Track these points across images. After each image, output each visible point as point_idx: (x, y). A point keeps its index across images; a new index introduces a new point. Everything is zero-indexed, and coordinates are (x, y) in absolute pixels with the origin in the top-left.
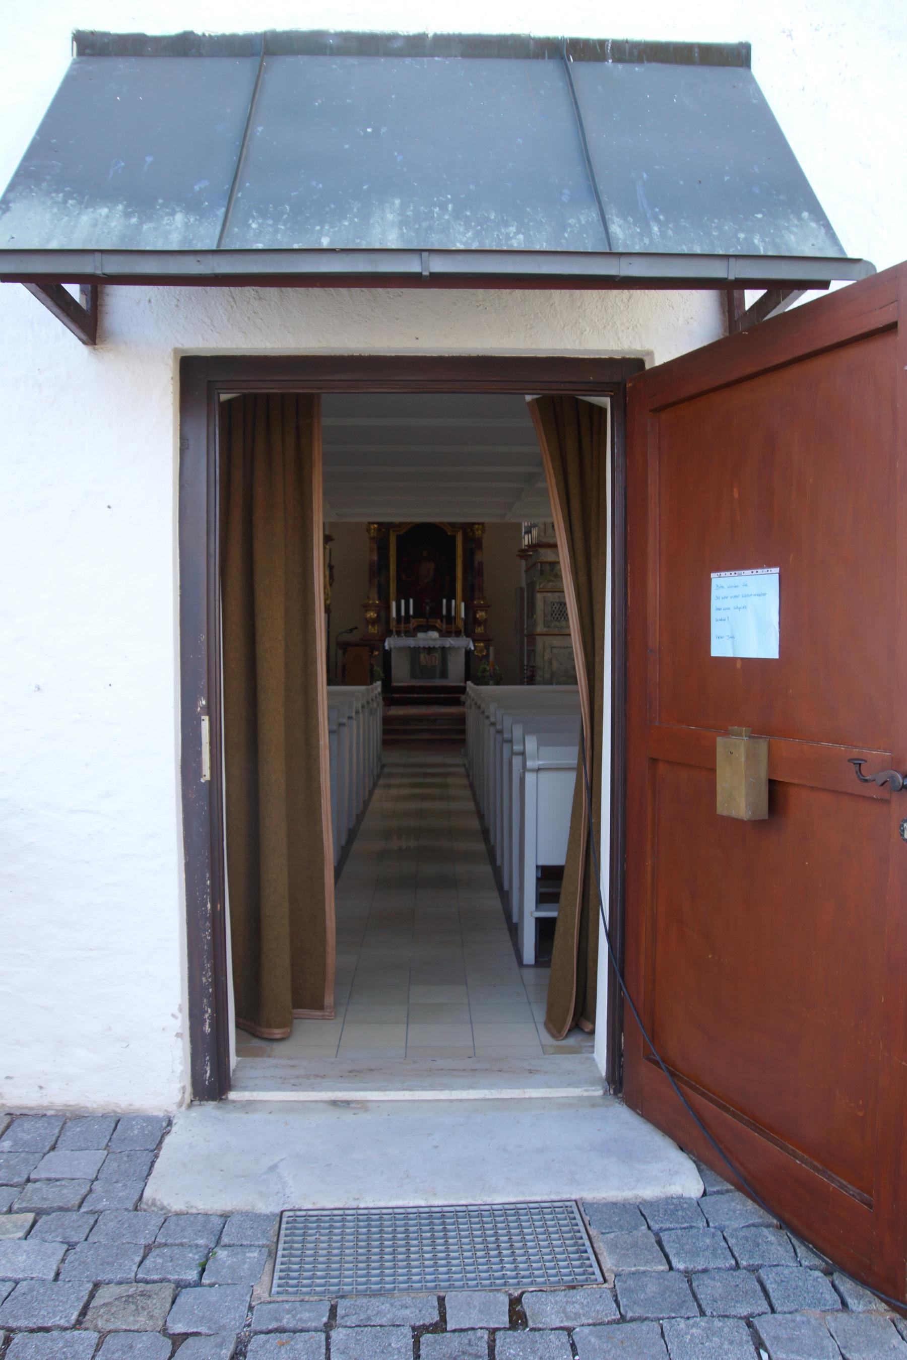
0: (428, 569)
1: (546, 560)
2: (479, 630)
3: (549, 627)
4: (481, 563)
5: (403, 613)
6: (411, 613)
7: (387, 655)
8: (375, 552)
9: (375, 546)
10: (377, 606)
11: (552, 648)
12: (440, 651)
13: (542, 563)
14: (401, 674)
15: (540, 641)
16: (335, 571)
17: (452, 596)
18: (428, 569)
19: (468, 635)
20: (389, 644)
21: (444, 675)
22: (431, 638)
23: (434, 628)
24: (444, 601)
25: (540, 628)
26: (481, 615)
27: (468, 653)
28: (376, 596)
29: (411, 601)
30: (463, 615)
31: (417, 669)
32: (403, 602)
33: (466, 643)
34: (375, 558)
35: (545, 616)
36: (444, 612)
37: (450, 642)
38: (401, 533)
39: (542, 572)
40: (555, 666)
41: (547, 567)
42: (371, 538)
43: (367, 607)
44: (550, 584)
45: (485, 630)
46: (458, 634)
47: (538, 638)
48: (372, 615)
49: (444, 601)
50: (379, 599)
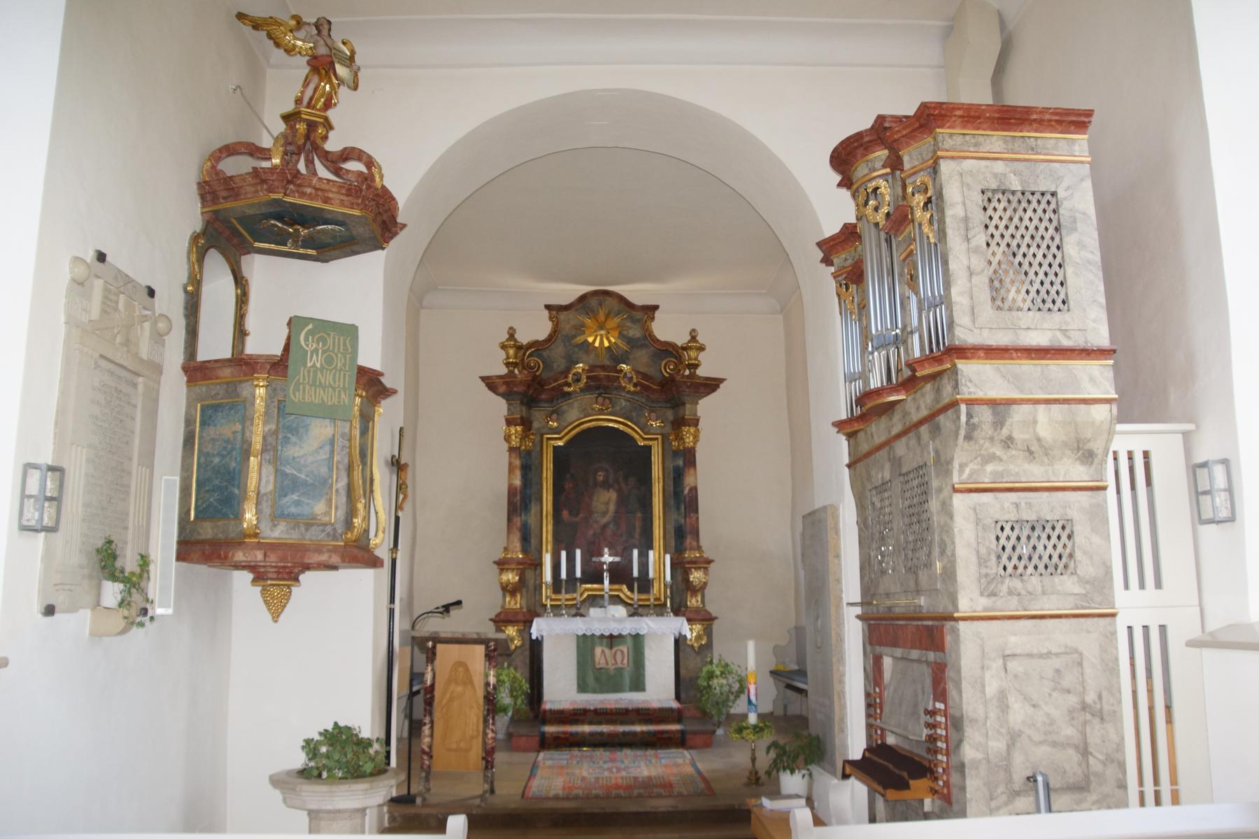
0: (605, 501)
1: (980, 395)
2: (693, 602)
4: (694, 490)
5: (564, 575)
6: (578, 574)
7: (535, 647)
8: (518, 473)
9: (517, 462)
10: (519, 562)
11: (1005, 657)
12: (630, 642)
13: (970, 402)
14: (561, 688)
17: (647, 544)
18: (605, 501)
19: (677, 612)
20: (538, 630)
22: (611, 619)
24: (635, 552)
25: (968, 600)
26: (696, 576)
27: (679, 642)
29: (578, 553)
30: (668, 578)
31: (589, 676)
32: (564, 554)
34: (517, 482)
35: (982, 562)
36: (636, 574)
38: (561, 443)
40: (1018, 713)
42: (511, 449)
43: (502, 565)
44: (990, 468)
45: (703, 602)
46: (659, 609)
47: (962, 625)
48: (511, 577)
49: (635, 552)
50: (524, 551)
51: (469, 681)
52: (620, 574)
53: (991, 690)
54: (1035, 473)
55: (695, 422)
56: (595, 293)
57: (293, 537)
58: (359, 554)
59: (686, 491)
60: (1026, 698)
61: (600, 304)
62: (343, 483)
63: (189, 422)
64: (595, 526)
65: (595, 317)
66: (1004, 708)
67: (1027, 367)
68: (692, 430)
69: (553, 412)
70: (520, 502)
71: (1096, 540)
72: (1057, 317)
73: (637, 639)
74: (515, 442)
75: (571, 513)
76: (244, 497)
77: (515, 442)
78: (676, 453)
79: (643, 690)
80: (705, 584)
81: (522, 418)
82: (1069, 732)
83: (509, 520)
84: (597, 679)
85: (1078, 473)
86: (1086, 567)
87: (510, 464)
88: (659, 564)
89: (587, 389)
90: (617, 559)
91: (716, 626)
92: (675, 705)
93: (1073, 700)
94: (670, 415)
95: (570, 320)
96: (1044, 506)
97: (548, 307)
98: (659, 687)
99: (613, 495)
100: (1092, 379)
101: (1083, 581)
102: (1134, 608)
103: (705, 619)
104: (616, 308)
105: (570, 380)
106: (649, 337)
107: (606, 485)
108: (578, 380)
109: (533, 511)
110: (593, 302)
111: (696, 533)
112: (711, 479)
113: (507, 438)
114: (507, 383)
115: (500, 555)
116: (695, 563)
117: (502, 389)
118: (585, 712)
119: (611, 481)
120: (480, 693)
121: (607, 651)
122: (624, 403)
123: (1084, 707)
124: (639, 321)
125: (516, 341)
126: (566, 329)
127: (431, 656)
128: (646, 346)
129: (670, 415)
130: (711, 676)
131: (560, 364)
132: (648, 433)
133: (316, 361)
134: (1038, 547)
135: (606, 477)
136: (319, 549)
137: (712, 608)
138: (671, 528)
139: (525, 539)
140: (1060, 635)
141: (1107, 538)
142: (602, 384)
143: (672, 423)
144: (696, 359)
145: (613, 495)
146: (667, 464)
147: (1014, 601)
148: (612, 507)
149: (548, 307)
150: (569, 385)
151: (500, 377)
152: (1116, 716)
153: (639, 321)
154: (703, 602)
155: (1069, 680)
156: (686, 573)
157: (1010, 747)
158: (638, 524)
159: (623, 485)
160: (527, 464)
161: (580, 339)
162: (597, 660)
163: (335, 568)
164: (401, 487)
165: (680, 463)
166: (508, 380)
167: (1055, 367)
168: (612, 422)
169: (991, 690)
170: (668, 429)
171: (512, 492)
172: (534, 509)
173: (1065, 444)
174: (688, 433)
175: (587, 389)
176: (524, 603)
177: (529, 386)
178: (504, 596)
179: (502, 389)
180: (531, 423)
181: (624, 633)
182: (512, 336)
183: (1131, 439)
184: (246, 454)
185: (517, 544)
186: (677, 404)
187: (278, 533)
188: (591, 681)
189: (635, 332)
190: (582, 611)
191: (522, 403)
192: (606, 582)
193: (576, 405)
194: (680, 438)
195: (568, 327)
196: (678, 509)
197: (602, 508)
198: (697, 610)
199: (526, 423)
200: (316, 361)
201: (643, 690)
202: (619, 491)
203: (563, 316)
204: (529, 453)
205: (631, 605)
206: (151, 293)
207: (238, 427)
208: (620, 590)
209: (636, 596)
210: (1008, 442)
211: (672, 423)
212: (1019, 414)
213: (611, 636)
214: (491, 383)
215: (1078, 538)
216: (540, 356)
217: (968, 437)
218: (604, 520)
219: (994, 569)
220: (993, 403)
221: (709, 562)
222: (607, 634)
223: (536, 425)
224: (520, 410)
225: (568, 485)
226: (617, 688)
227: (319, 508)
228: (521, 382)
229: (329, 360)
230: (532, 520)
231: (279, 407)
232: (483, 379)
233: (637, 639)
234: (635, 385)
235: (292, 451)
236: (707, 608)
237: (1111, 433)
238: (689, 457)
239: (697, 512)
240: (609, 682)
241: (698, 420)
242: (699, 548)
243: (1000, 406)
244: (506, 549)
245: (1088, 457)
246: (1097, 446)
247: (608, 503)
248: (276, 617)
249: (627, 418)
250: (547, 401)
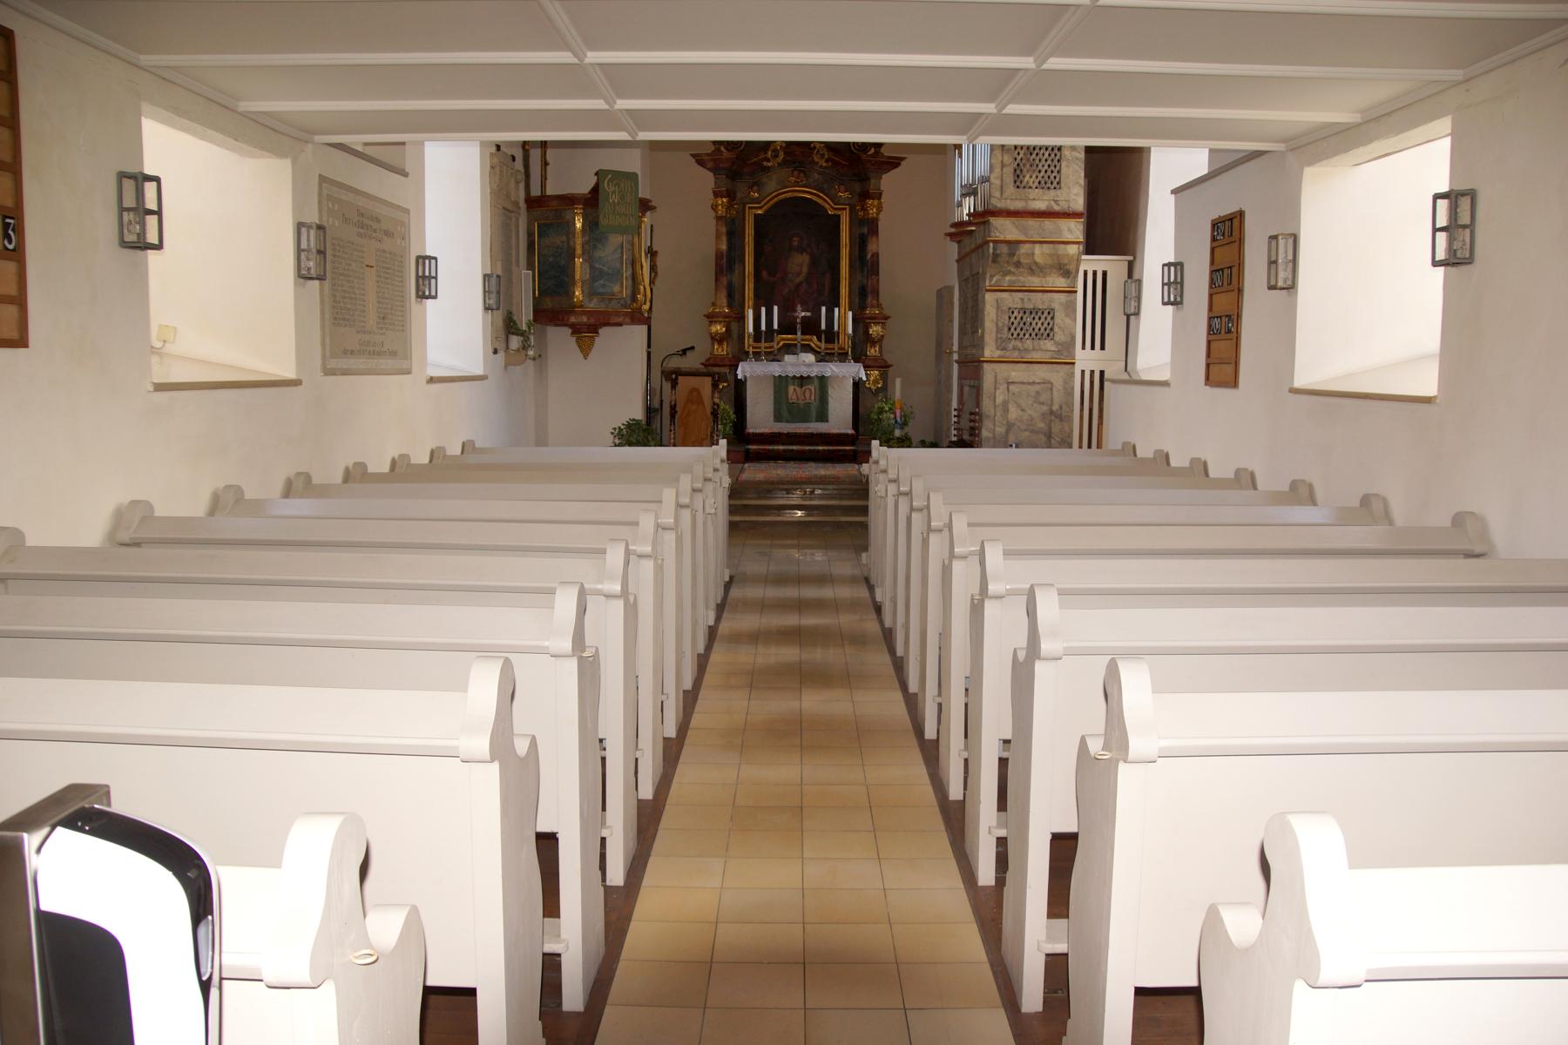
0: (799, 263)
2: (873, 352)
3: (1004, 349)
4: (876, 255)
5: (763, 327)
7: (740, 387)
12: (816, 382)
13: (995, 242)
14: (760, 416)
15: (989, 372)
16: (660, 261)
17: (834, 302)
18: (799, 263)
19: (856, 361)
21: (823, 416)
22: (803, 363)
23: (807, 348)
25: (990, 352)
26: (875, 330)
27: (857, 385)
28: (725, 301)
30: (850, 330)
31: (783, 409)
33: (856, 370)
34: (724, 247)
35: (999, 330)
36: (823, 327)
37: (832, 369)
39: (996, 257)
40: (1013, 413)
41: (1004, 249)
42: (718, 218)
43: (711, 318)
46: (842, 357)
47: (985, 365)
48: (718, 328)
50: (729, 306)
51: (700, 401)
52: (810, 327)
53: (1000, 399)
54: (1035, 281)
55: (879, 196)
57: (602, 307)
58: (637, 317)
60: (1018, 406)
62: (630, 272)
63: (530, 234)
66: (1006, 410)
67: (1032, 223)
69: (755, 184)
70: (727, 264)
71: (1068, 321)
72: (1052, 193)
74: (721, 211)
76: (574, 283)
77: (721, 211)
78: (862, 222)
82: (1042, 425)
85: (1061, 282)
86: (1060, 336)
88: (845, 320)
89: (784, 163)
91: (891, 371)
92: (850, 431)
93: (1045, 408)
94: (857, 187)
96: (1039, 301)
98: (839, 416)
100: (1070, 230)
101: (1057, 344)
102: (1086, 360)
103: (883, 366)
107: (801, 250)
111: (876, 293)
112: (890, 246)
113: (715, 207)
117: (710, 165)
118: (780, 434)
120: (709, 410)
123: (1052, 412)
127: (674, 384)
130: (881, 411)
133: (615, 198)
134: (1033, 324)
136: (617, 314)
137: (888, 358)
139: (730, 296)
140: (1041, 373)
141: (1075, 320)
147: (1016, 353)
148: (805, 269)
152: (1070, 419)
155: (1043, 398)
156: (867, 328)
157: (1008, 431)
160: (733, 232)
163: (620, 325)
164: (653, 268)
165: (865, 230)
167: (1048, 224)
168: (807, 193)
169: (999, 399)
171: (719, 255)
173: (1052, 266)
175: (784, 163)
179: (710, 165)
183: (1093, 263)
184: (572, 256)
186: (863, 178)
187: (593, 305)
188: (785, 414)
194: (864, 209)
198: (875, 359)
199: (730, 195)
200: (615, 198)
204: (733, 220)
206: (514, 158)
207: (564, 238)
209: (823, 345)
210: (1018, 264)
212: (1024, 249)
215: (1057, 320)
217: (994, 261)
218: (798, 280)
219: (1005, 334)
220: (1008, 242)
223: (739, 195)
226: (805, 419)
227: (616, 289)
229: (622, 198)
230: (735, 278)
231: (592, 224)
233: (823, 380)
235: (599, 253)
237: (1079, 261)
238: (873, 227)
240: (800, 414)
242: (879, 306)
243: (1013, 244)
244: (714, 304)
245: (1067, 273)
246: (1072, 267)
248: (586, 356)
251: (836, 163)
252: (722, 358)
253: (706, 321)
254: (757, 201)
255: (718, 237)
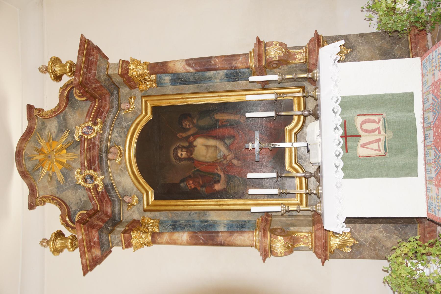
0: (205, 149)
4: (188, 62)
6: (274, 175)
10: (265, 236)
18: (205, 149)
22: (321, 140)
24: (248, 115)
26: (274, 53)
31: (395, 161)
32: (251, 191)
33: (328, 54)
34: (184, 236)
36: (272, 114)
38: (151, 193)
48: (279, 243)
49: (248, 115)
55: (125, 63)
56: (19, 163)
59: (191, 70)
61: (30, 158)
64: (229, 158)
65: (41, 163)
68: (132, 67)
73: (347, 104)
75: (218, 182)
78: (159, 83)
79: (412, 94)
80: (281, 44)
81: (124, 232)
83: (222, 244)
84: (400, 151)
87: (168, 243)
90: (257, 134)
94: (124, 90)
95: (44, 188)
97: (31, 207)
99: (200, 143)
104: (33, 144)
105: (91, 186)
106: (57, 113)
107: (190, 148)
108: (92, 177)
109: (215, 218)
110: (28, 165)
114: (90, 248)
115: (256, 253)
116: (260, 56)
119: (186, 144)
121: (363, 140)
122: (115, 134)
124: (43, 123)
125: (51, 240)
126: (51, 189)
128: (65, 115)
129: (124, 90)
131: (82, 195)
132: (138, 111)
135: (182, 148)
138: (229, 85)
142: (96, 157)
143: (132, 88)
144: (65, 65)
145: (200, 142)
146: (169, 92)
148: (212, 142)
149: (31, 207)
150: (96, 187)
151: (82, 254)
153: (43, 123)
154: (300, 48)
158: (225, 117)
159: (191, 132)
161: (60, 177)
162: (374, 153)
165: (167, 78)
166: (86, 247)
170: (136, 92)
171: (195, 241)
172: (212, 217)
174: (135, 71)
176: (305, 229)
177: (93, 227)
178: (298, 249)
179: (97, 252)
180: (134, 221)
181: (341, 121)
182: (48, 242)
185: (246, 237)
188: (401, 160)
189: (53, 126)
190: (312, 170)
191: (111, 232)
192: (282, 145)
193: (117, 179)
195: (50, 188)
196: (210, 79)
197: (211, 150)
199: (135, 225)
201: (412, 94)
202: (196, 135)
203: (41, 193)
205: (305, 117)
208: (291, 131)
209: (296, 112)
211: (132, 88)
213: (345, 136)
214: (88, 266)
216: (75, 213)
218: (223, 150)
221: (259, 42)
222: (341, 141)
223: (136, 216)
224: (118, 235)
225: (191, 185)
228: (86, 235)
232: (85, 273)
234: (95, 124)
236: (305, 44)
238: (159, 68)
239: (210, 58)
241: (123, 61)
247: (207, 147)
249: (128, 130)
250: (113, 207)
251: (99, 113)
252: (315, 237)
253: (271, 259)
254: (140, 201)
255: (175, 243)
